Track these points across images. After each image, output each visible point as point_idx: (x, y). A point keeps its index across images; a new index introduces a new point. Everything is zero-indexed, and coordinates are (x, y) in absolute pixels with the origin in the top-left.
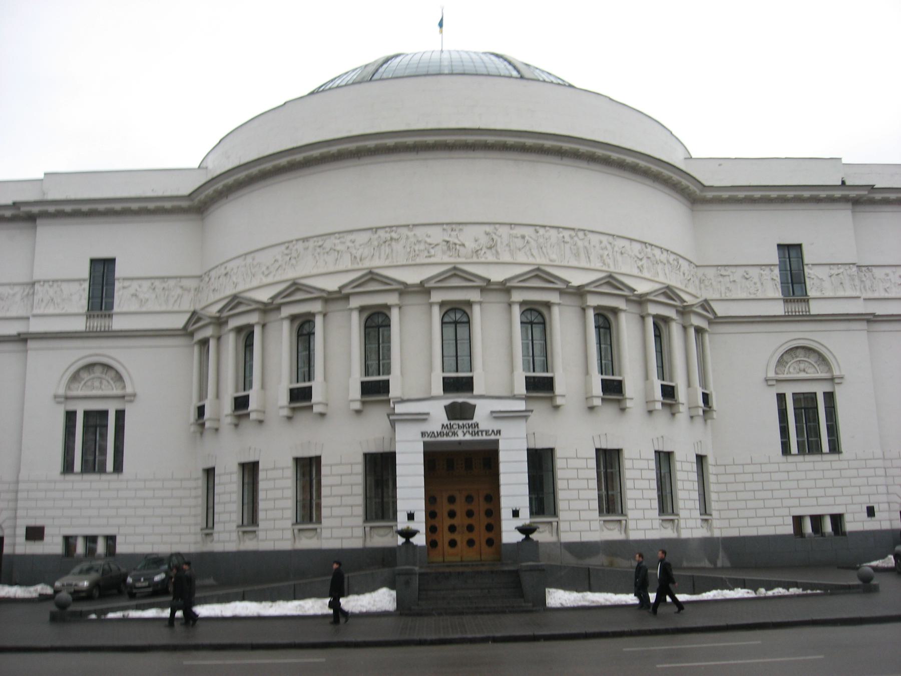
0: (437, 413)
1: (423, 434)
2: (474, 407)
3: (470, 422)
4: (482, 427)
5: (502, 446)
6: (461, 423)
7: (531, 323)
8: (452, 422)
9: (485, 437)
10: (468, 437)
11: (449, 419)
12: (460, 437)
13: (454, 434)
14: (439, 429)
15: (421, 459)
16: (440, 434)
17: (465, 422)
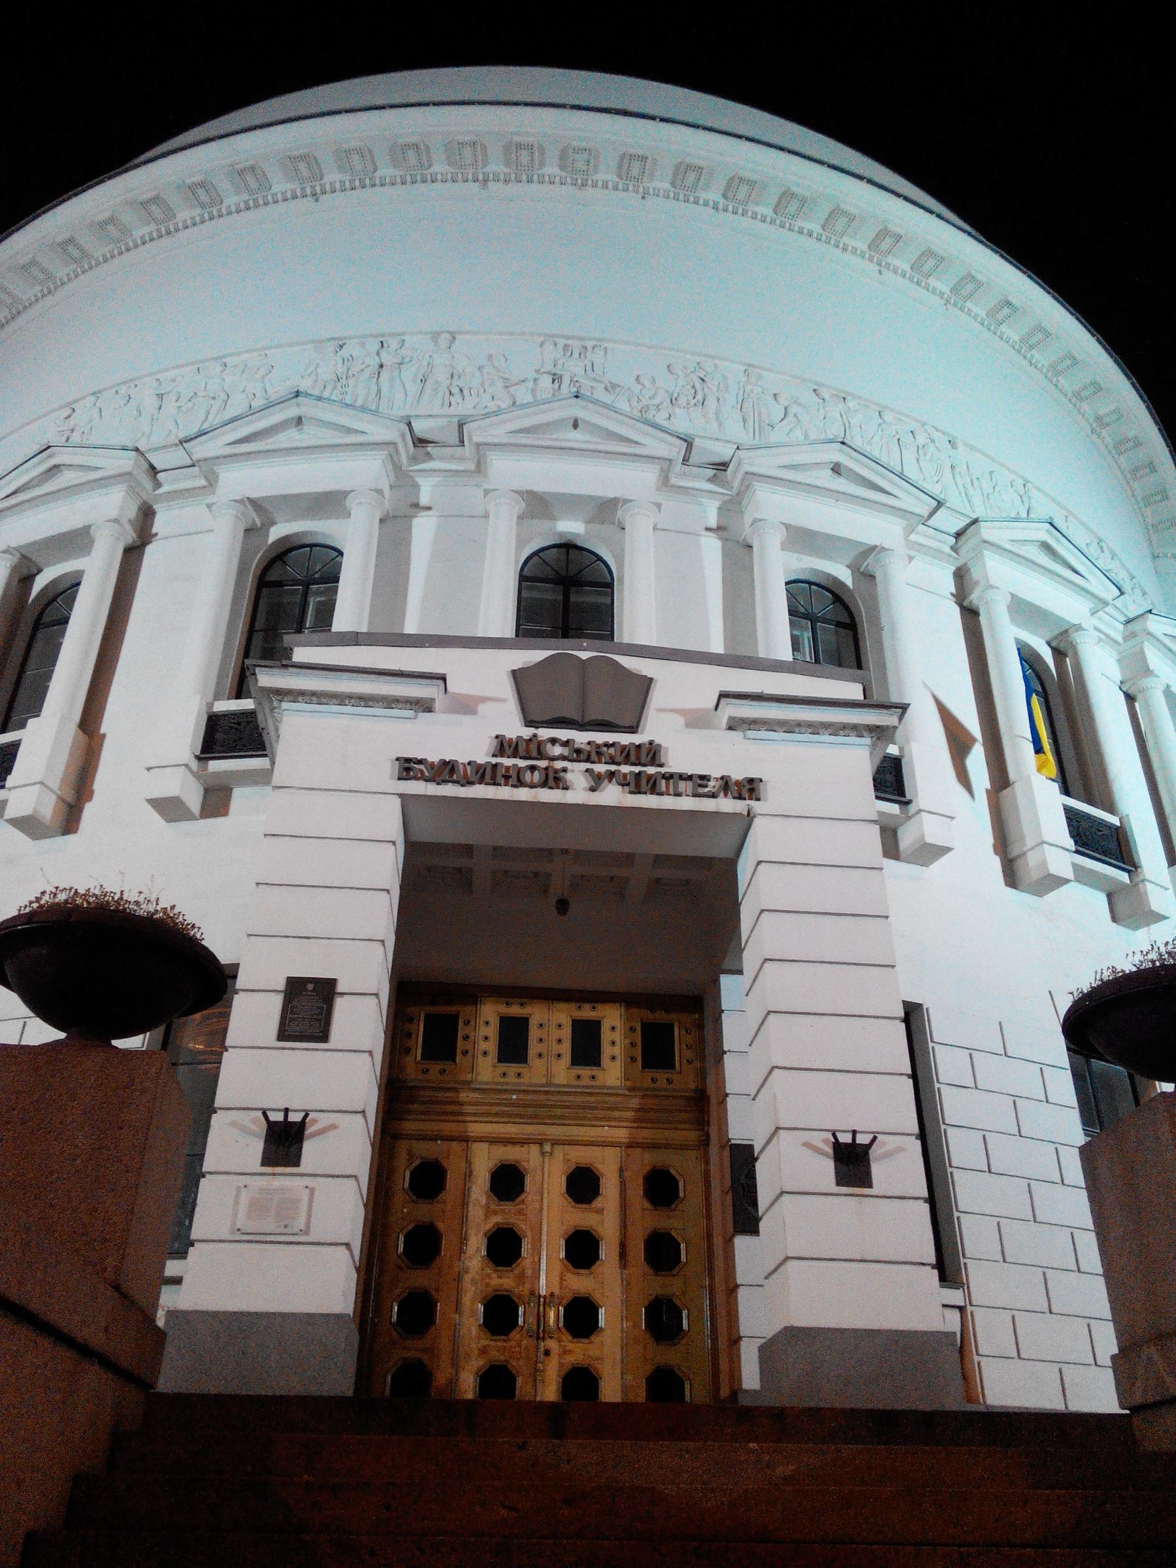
0: (481, 707)
1: (408, 768)
2: (648, 683)
3: (625, 739)
4: (675, 763)
5: (764, 839)
6: (581, 738)
7: (813, 619)
8: (545, 733)
9: (687, 803)
10: (612, 796)
11: (529, 723)
12: (578, 790)
13: (554, 780)
14: (483, 756)
15: (386, 867)
16: (485, 774)
17: (600, 737)
